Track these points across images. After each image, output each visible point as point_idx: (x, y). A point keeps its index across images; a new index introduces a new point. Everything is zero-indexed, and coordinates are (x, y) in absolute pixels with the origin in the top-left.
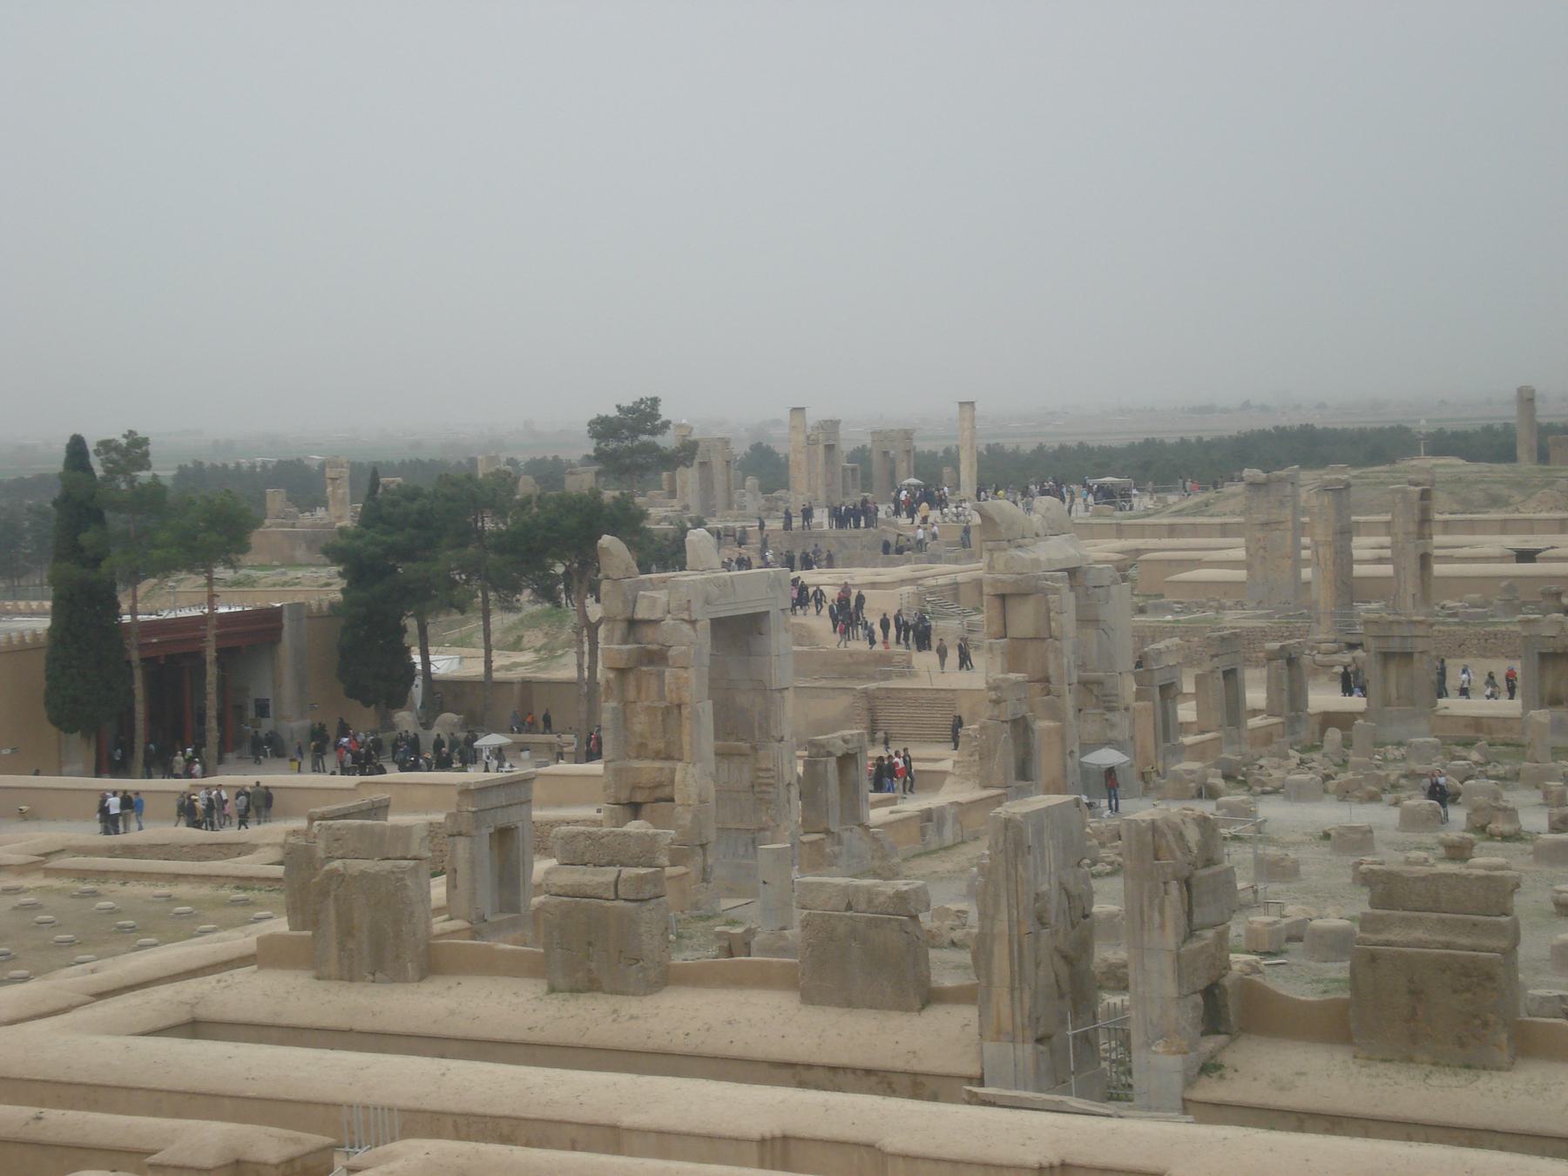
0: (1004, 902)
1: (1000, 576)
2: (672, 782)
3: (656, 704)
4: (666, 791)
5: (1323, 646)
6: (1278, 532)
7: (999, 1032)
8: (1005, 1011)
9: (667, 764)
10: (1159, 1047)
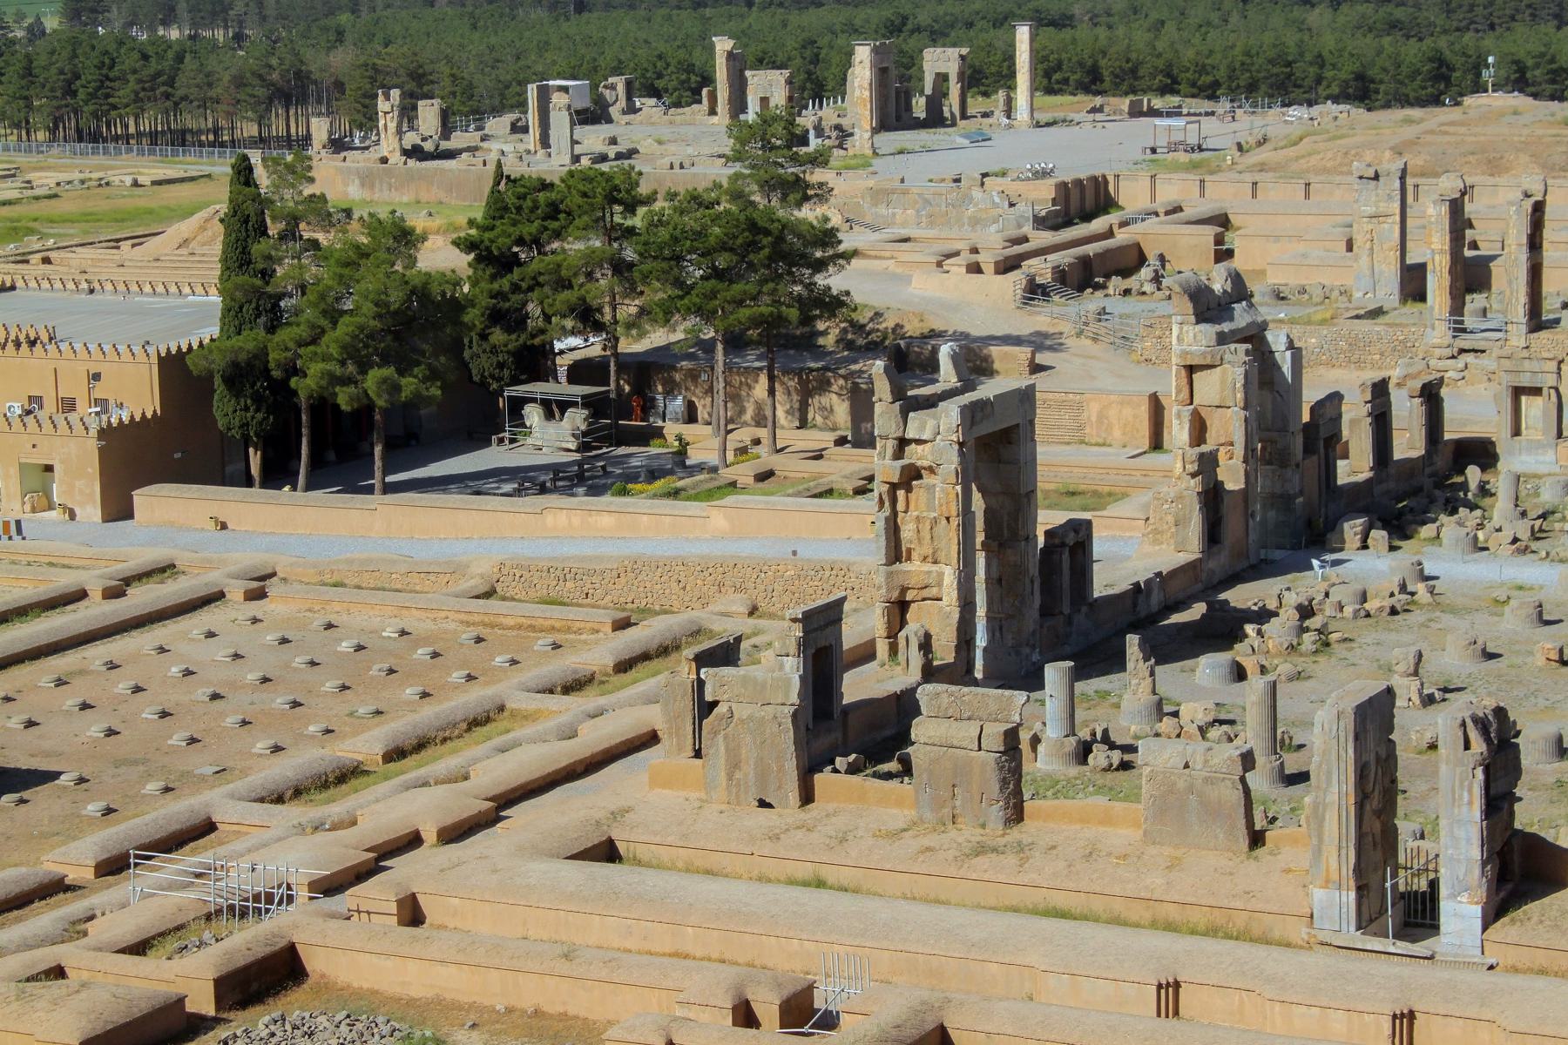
0: (1335, 777)
1: (1188, 348)
2: (940, 584)
3: (925, 514)
4: (934, 592)
5: (1438, 352)
6: (1386, 226)
7: (1327, 881)
8: (1334, 865)
9: (935, 568)
10: (1464, 898)
